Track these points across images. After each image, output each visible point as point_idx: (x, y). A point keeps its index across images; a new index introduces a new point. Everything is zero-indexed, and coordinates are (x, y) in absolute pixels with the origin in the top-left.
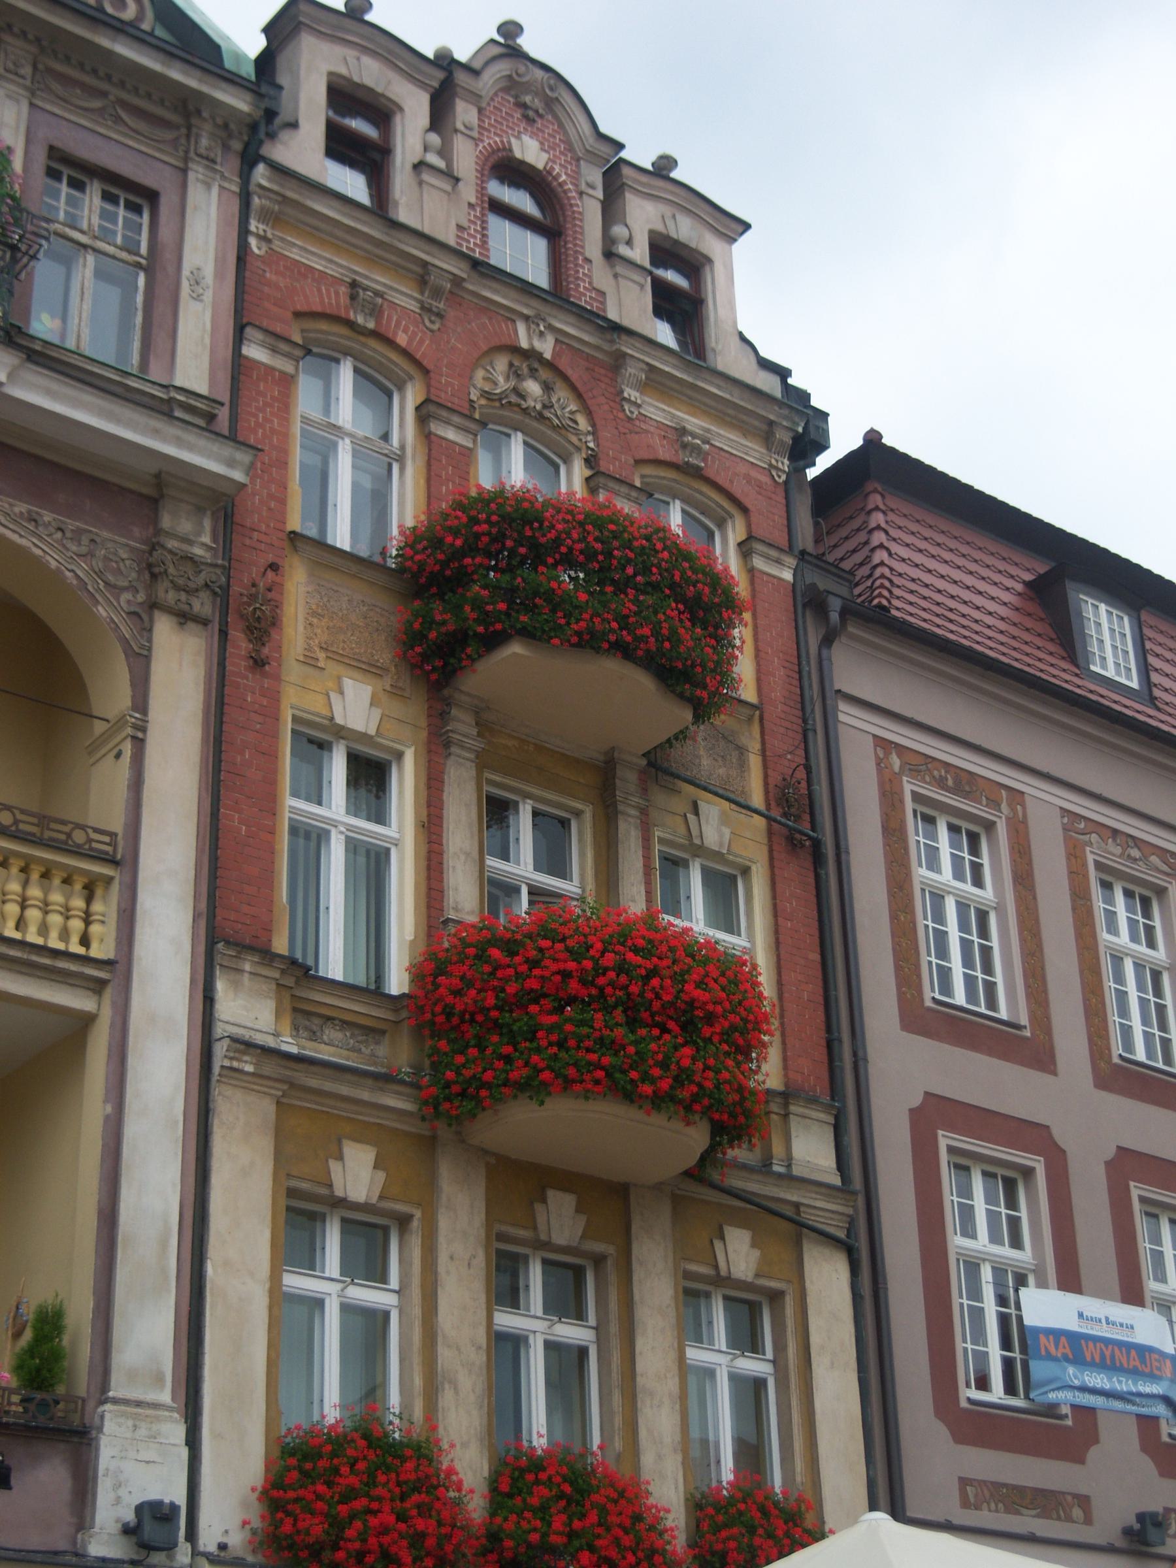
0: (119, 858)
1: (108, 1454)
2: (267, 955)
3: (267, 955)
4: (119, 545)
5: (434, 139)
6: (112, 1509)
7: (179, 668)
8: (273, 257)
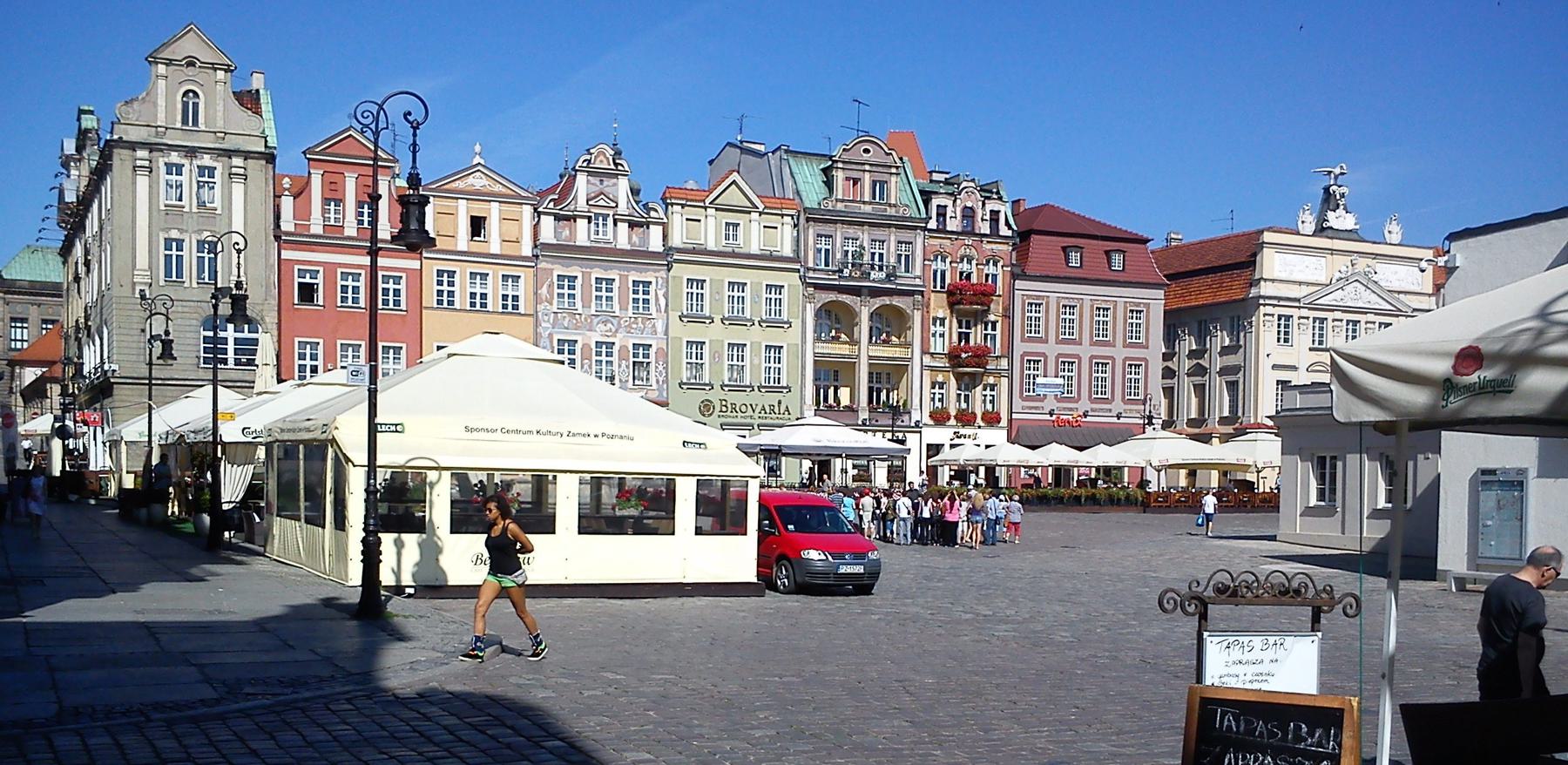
7: (917, 316)
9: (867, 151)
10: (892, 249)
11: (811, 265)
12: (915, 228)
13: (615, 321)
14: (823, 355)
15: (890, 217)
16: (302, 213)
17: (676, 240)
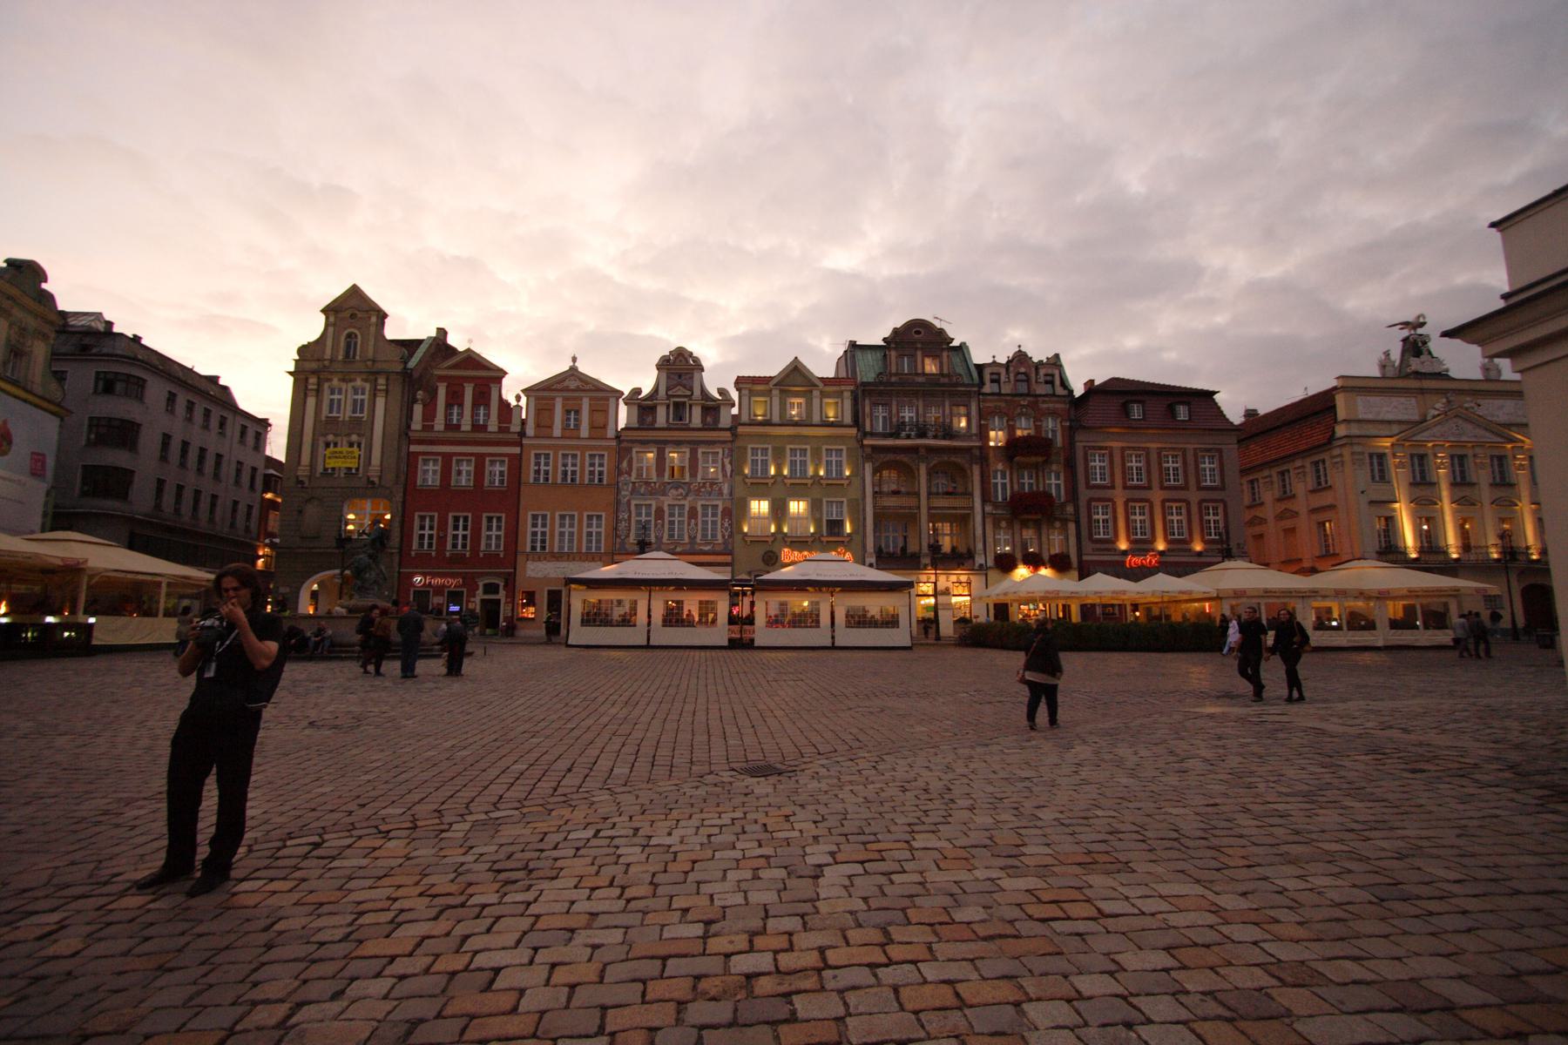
0: (972, 494)
7: (976, 470)
9: (918, 333)
12: (968, 394)
15: (944, 385)
16: (429, 415)
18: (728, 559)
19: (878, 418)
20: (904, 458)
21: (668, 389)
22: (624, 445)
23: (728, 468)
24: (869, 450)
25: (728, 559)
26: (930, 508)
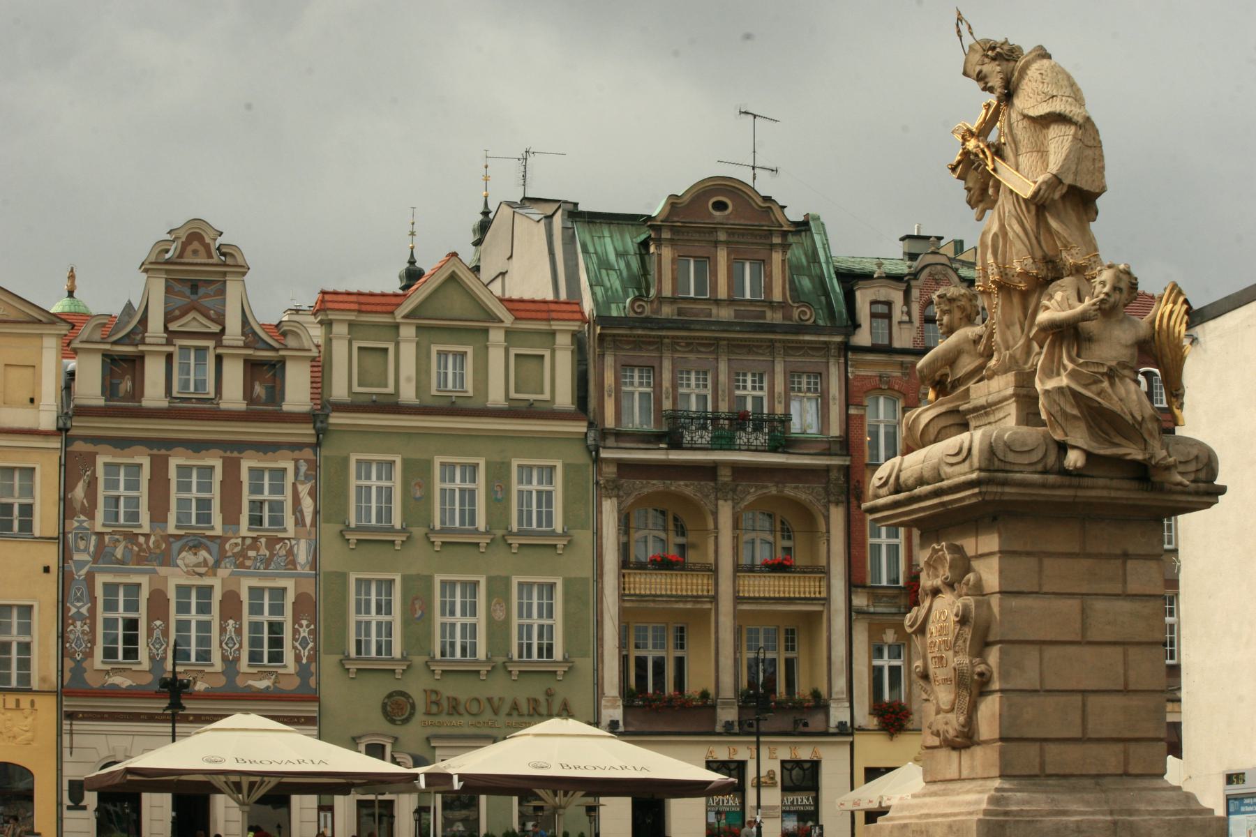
0: (825, 572)
1: (832, 711)
2: (864, 587)
3: (864, 587)
4: (818, 487)
5: (905, 309)
6: (833, 723)
7: (837, 516)
8: (857, 377)
9: (720, 206)
10: (779, 387)
11: (610, 422)
13: (214, 547)
14: (641, 597)
15: (772, 328)
17: (339, 391)
18: (310, 709)
19: (630, 402)
20: (685, 487)
21: (169, 318)
22: (79, 446)
23: (308, 505)
24: (610, 471)
25: (310, 709)
26: (738, 599)
